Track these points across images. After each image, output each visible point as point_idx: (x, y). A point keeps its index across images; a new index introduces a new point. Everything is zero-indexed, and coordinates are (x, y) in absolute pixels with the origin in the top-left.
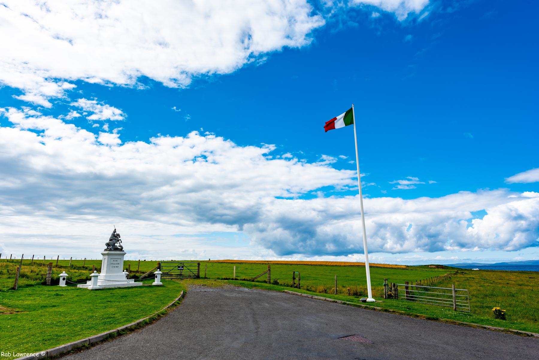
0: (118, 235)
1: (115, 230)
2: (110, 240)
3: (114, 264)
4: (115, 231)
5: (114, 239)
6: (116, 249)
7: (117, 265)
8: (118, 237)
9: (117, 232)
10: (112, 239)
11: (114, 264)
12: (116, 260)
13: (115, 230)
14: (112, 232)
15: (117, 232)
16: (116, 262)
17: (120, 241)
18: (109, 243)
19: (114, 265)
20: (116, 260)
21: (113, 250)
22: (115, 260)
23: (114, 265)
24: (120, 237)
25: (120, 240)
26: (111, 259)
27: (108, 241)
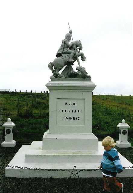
0: (78, 45)
1: (71, 32)
4: (69, 37)
5: (66, 53)
6: (73, 76)
7: (76, 115)
8: (78, 47)
10: (61, 52)
13: (71, 32)
14: (63, 38)
15: (75, 38)
17: (80, 58)
18: (55, 61)
19: (68, 115)
21: (64, 77)
23: (68, 115)
24: (81, 49)
25: (82, 55)
26: (59, 100)
27: (53, 58)
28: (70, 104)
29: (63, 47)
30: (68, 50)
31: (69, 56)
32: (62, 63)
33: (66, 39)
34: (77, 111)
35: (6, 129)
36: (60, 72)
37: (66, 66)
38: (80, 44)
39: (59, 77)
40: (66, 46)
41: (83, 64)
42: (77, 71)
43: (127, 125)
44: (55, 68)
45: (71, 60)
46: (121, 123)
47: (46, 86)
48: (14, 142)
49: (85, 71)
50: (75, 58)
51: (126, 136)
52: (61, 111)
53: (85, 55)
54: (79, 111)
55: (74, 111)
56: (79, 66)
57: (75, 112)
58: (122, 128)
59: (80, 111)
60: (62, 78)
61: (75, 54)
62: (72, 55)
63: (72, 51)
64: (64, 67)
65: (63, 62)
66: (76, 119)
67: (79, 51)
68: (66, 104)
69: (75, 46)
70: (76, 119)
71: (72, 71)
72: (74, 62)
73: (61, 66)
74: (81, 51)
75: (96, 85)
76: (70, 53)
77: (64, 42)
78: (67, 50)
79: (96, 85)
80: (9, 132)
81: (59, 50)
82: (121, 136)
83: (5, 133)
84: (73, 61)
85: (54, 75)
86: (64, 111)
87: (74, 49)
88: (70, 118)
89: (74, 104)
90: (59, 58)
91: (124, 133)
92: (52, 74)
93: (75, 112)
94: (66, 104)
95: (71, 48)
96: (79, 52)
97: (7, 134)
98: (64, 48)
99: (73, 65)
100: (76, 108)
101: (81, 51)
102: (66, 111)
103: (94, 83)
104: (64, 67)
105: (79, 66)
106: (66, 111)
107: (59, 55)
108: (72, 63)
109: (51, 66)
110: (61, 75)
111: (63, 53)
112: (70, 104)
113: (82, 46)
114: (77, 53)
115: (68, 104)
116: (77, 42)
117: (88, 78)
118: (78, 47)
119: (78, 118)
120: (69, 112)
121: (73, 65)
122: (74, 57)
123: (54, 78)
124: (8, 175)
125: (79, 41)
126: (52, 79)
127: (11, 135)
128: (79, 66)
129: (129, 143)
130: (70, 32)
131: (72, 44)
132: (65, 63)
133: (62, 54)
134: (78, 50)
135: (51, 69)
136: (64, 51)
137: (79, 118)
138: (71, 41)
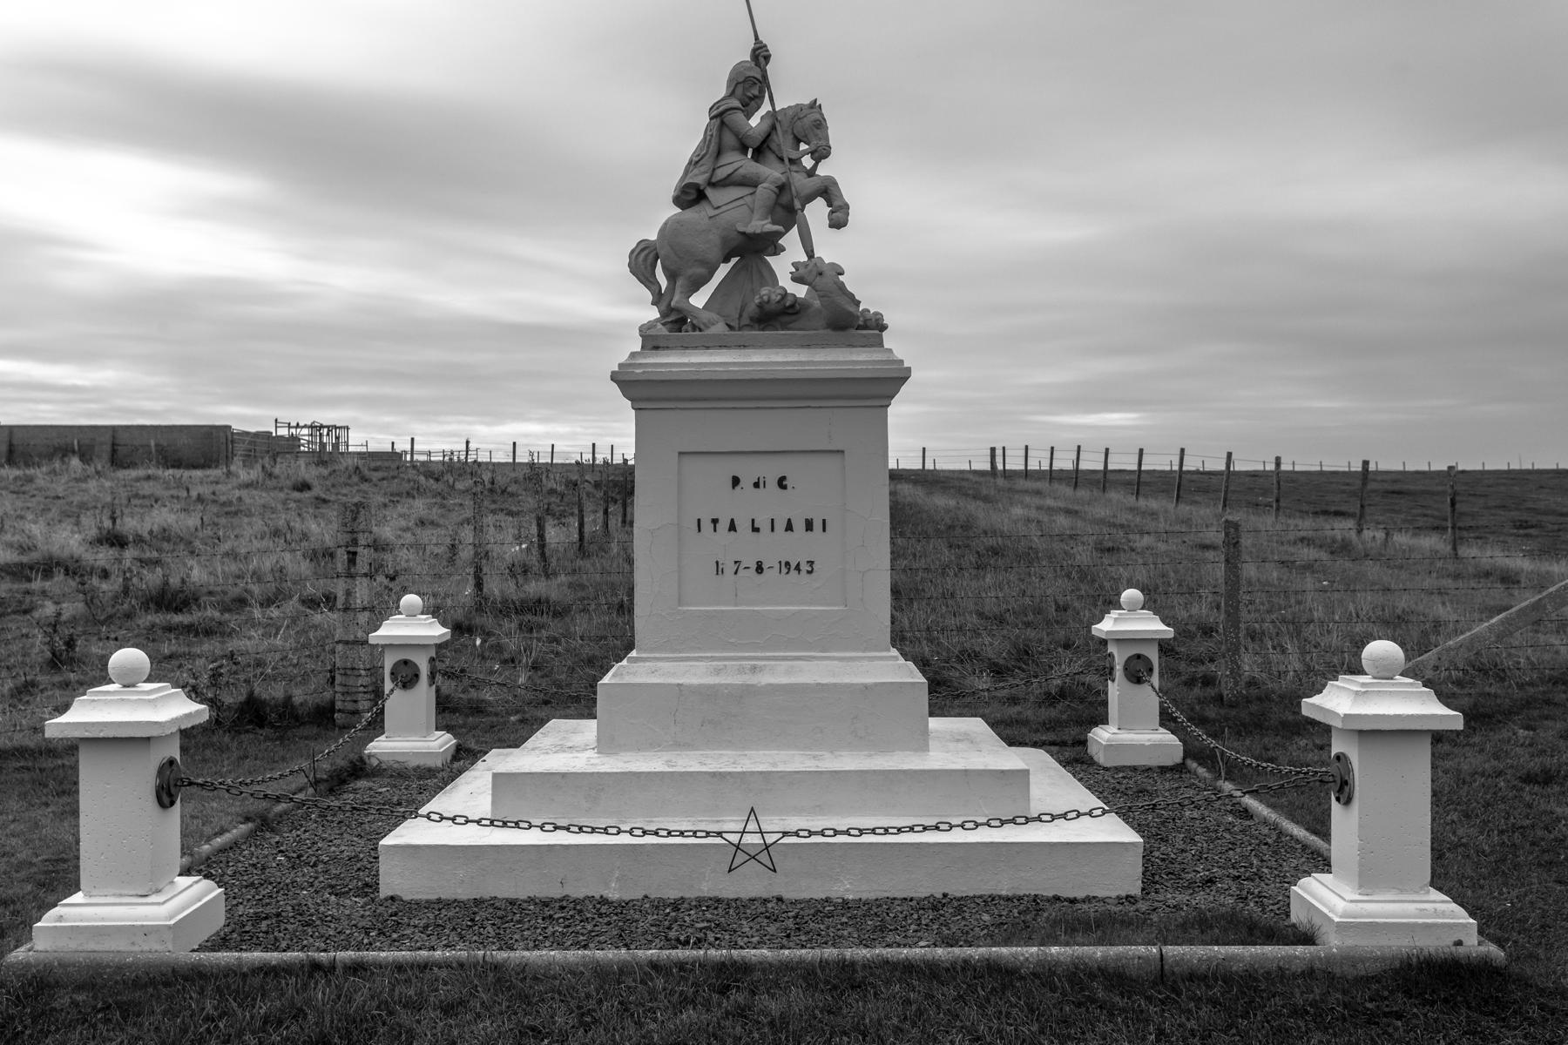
1: (761, 55)
2: (679, 201)
3: (743, 526)
7: (798, 546)
8: (803, 147)
9: (786, 94)
10: (700, 179)
11: (743, 526)
12: (770, 470)
13: (761, 55)
15: (786, 94)
16: (769, 505)
17: (816, 213)
20: (770, 470)
21: (719, 328)
22: (749, 470)
23: (747, 547)
24: (821, 154)
25: (828, 191)
26: (686, 459)
28: (756, 485)
29: (713, 147)
30: (745, 164)
31: (748, 199)
32: (710, 245)
33: (731, 94)
34: (799, 525)
35: (389, 662)
36: (699, 300)
37: (734, 260)
38: (820, 124)
39: (695, 328)
40: (729, 139)
41: (830, 247)
42: (801, 291)
43: (1152, 625)
44: (672, 276)
45: (761, 225)
46: (1114, 614)
47: (614, 377)
48: (440, 743)
49: (842, 287)
50: (787, 210)
51: (1148, 698)
52: (707, 526)
53: (848, 193)
54: (809, 525)
55: (781, 525)
56: (810, 254)
57: (789, 527)
58: (1123, 640)
59: (817, 525)
60: (713, 330)
61: (782, 188)
62: (765, 192)
63: (771, 172)
64: (723, 271)
65: (715, 238)
66: (798, 568)
67: (815, 167)
68: (736, 481)
69: (782, 141)
70: (793, 572)
71: (764, 291)
72: (781, 235)
73: (703, 262)
74: (822, 171)
75: (909, 369)
76: (751, 183)
77: (720, 117)
78: (736, 165)
79: (909, 369)
80: (406, 676)
81: (693, 164)
82: (1116, 690)
83: (388, 685)
84: (771, 227)
85: (664, 315)
86: (723, 525)
87: (781, 159)
88: (760, 569)
89: (782, 483)
90: (692, 214)
91: (1137, 672)
92: (653, 314)
93: (789, 527)
94: (736, 481)
95: (761, 150)
96: (811, 173)
97: (397, 692)
98: (719, 153)
99: (775, 254)
100: (794, 506)
101: (822, 171)
102: (732, 527)
103: (899, 354)
104: (723, 271)
105: (804, 258)
106: (732, 527)
107: (690, 196)
108: (769, 244)
109: (643, 262)
110: (706, 316)
111: (712, 184)
112: (756, 485)
113: (827, 139)
114: (800, 182)
115: (747, 482)
116: (798, 112)
117: (865, 327)
118: (803, 147)
119: (805, 567)
120: (756, 530)
121: (778, 250)
122: (776, 203)
123: (664, 331)
124: (394, 881)
125: (814, 105)
126: (651, 341)
127: (423, 696)
128: (810, 254)
129: (1167, 737)
130: (754, 51)
131: (766, 126)
132: (725, 240)
133: (709, 192)
134: (807, 162)
135: (647, 279)
136: (721, 173)
137: (811, 563)
138: (766, 108)
